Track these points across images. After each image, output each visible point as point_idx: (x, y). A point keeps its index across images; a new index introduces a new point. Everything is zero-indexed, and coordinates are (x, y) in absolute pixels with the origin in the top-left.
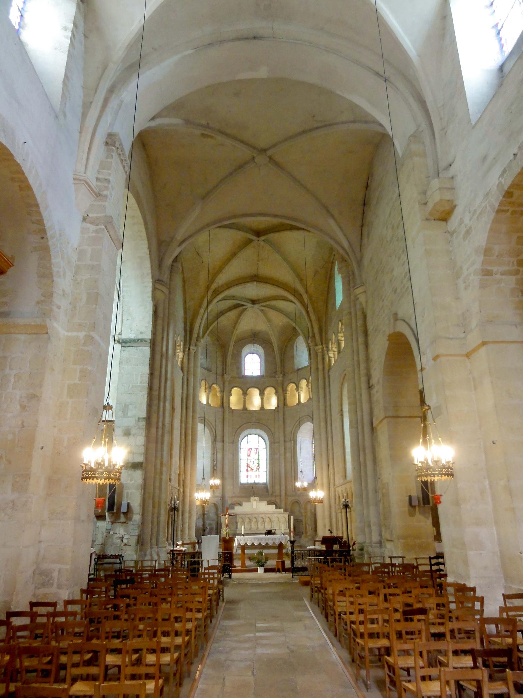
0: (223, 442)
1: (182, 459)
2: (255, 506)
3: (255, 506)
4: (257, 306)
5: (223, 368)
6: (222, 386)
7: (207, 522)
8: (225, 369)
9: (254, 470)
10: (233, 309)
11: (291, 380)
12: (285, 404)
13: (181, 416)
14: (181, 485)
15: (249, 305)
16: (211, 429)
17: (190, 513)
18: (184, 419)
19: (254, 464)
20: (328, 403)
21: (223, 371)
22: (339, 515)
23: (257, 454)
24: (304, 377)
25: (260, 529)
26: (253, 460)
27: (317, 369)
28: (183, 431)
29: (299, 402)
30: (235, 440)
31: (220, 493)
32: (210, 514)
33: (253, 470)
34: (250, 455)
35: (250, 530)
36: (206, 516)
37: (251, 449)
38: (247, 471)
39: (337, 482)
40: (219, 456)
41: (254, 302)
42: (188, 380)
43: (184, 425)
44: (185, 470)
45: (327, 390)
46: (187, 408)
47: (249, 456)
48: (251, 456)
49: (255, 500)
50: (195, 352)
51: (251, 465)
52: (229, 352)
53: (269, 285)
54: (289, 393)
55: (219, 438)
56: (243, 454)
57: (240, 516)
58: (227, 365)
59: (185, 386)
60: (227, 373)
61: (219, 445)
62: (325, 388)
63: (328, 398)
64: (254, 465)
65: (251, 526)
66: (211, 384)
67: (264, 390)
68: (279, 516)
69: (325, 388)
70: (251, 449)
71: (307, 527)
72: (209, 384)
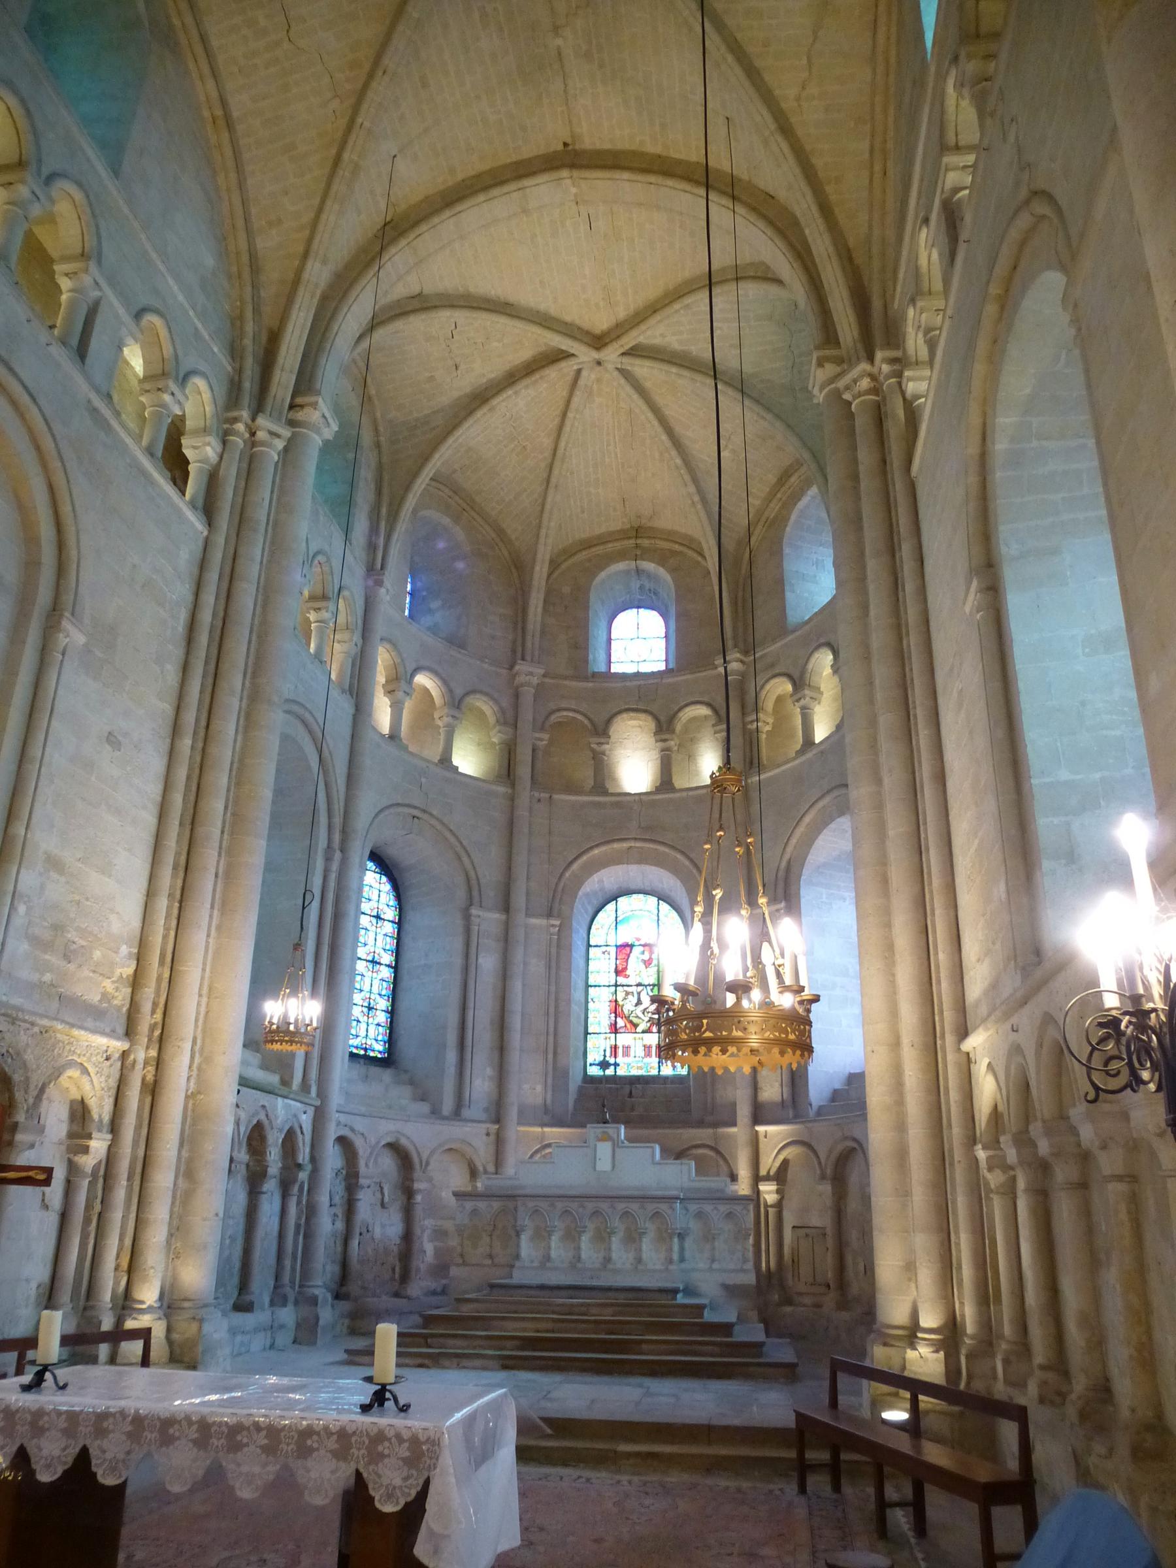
0: (506, 907)
1: (162, 903)
2: (604, 1164)
3: (604, 1163)
4: (611, 355)
5: (514, 642)
6: (505, 703)
7: (425, 1225)
8: (519, 642)
9: (639, 1029)
10: (522, 378)
11: (772, 665)
12: (753, 762)
13: (178, 709)
14: (143, 1027)
15: (585, 355)
16: (459, 858)
17: (188, 1171)
18: (190, 717)
19: (639, 1003)
20: (912, 614)
21: (514, 651)
22: (997, 1208)
23: (653, 970)
24: (822, 640)
25: (619, 1266)
26: (633, 989)
27: (855, 477)
28: (181, 773)
29: (808, 742)
30: (556, 905)
31: (486, 1110)
32: (443, 1194)
33: (636, 1026)
34: (625, 969)
35: (573, 1266)
36: (418, 1198)
37: (631, 946)
38: (614, 1029)
39: (975, 988)
40: (488, 962)
41: (598, 341)
42: (234, 559)
43: (186, 743)
44: (174, 961)
45: (906, 551)
46: (215, 676)
47: (618, 972)
48: (628, 973)
49: (605, 1138)
50: (286, 449)
51: (628, 1006)
52: (535, 583)
53: (626, 175)
54: (771, 720)
55: (491, 894)
56: (601, 967)
57: (531, 1204)
58: (530, 627)
59: (213, 576)
60: (528, 658)
61: (488, 919)
62: (892, 549)
63: (910, 587)
64: (642, 1007)
65: (579, 1248)
66: (459, 692)
67: (672, 718)
68: (708, 1208)
69: (892, 549)
70: (631, 946)
71: (849, 1259)
72: (451, 691)
